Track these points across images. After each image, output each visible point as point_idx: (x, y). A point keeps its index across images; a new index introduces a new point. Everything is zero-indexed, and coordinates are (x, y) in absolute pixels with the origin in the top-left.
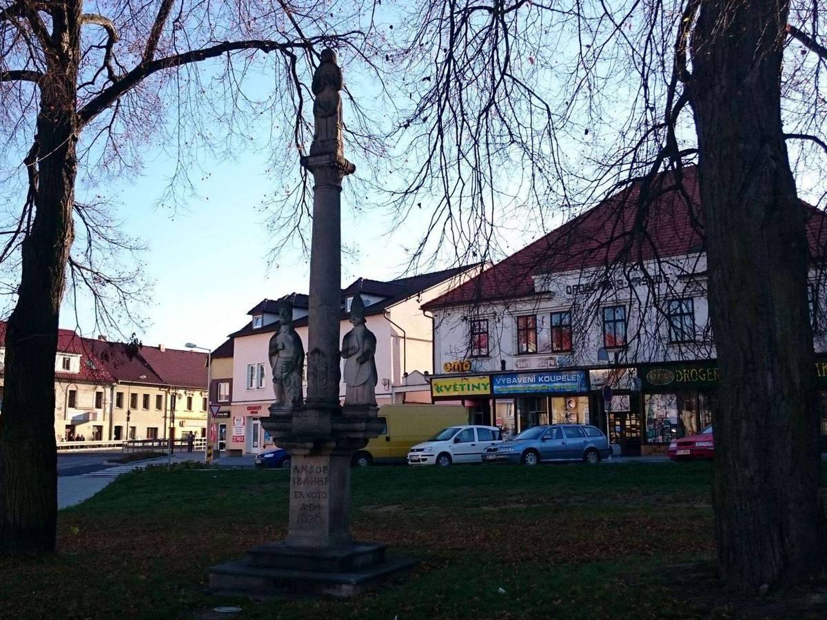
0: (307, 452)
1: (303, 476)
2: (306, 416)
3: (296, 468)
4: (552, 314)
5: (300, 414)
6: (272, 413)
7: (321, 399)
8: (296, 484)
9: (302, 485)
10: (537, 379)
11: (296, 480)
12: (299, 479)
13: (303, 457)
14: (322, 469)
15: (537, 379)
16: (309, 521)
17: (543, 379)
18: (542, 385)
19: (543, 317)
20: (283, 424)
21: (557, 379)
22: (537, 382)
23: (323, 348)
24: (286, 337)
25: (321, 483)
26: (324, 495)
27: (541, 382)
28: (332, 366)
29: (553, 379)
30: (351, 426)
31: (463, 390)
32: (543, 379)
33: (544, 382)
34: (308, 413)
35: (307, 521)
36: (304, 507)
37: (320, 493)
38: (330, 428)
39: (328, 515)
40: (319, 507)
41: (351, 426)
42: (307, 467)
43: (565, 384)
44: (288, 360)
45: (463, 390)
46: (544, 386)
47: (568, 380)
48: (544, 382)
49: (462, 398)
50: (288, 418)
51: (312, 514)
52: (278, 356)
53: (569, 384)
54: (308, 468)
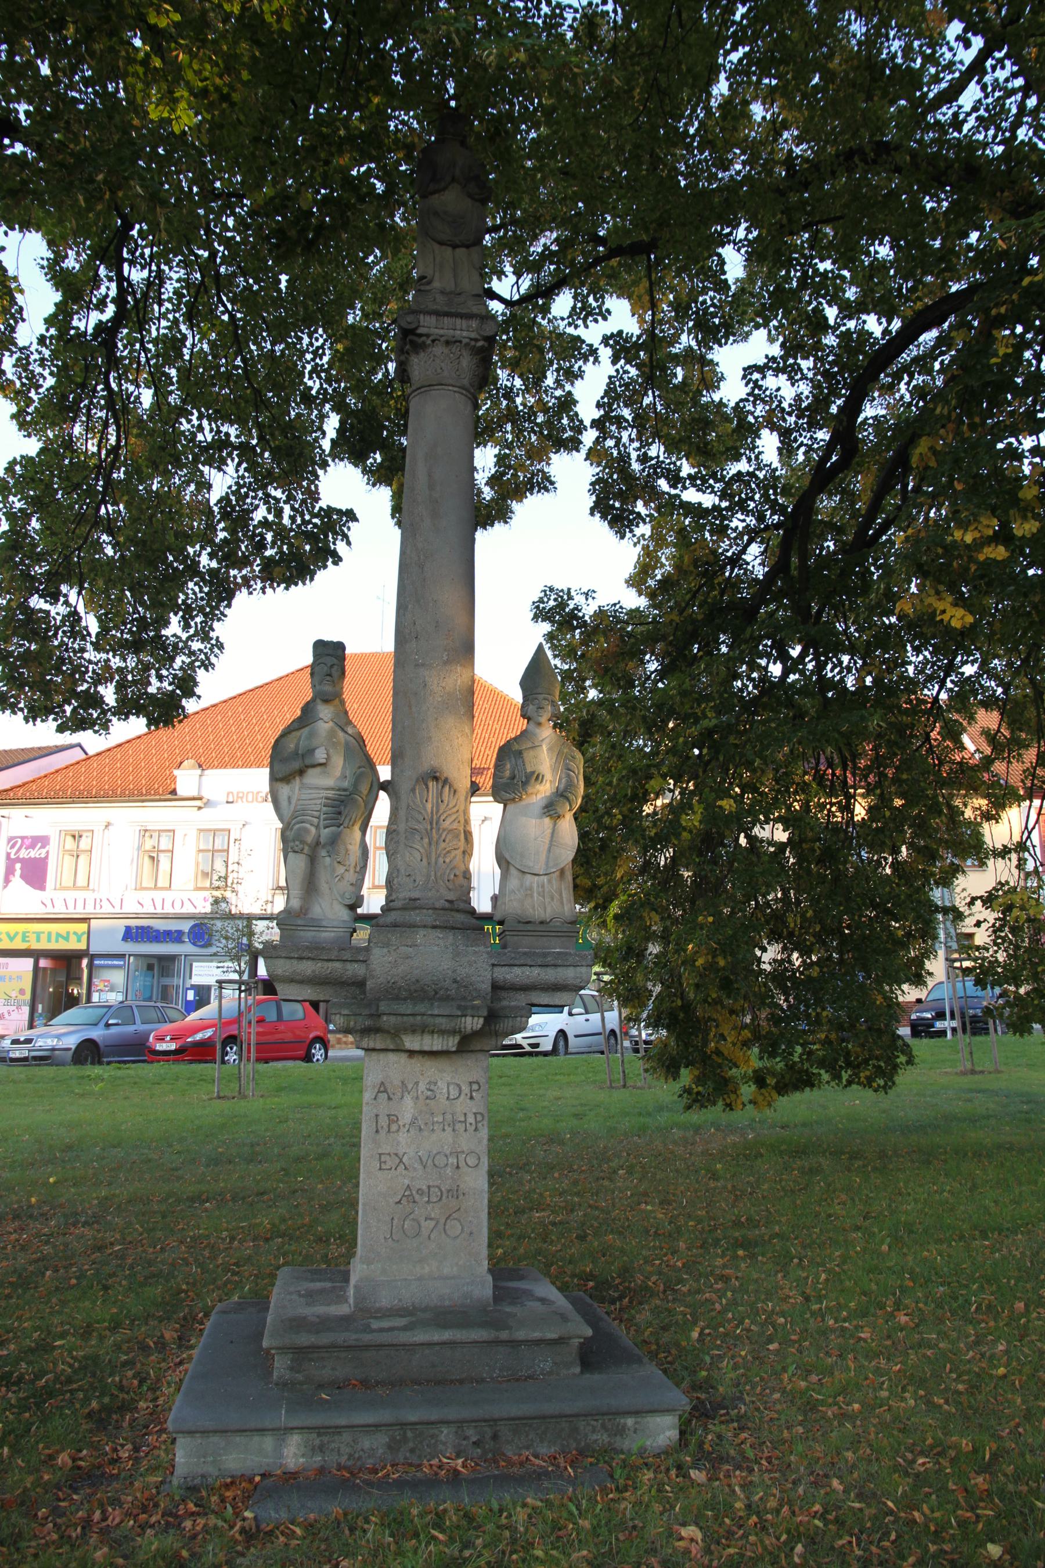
1: (407, 1108)
3: (382, 1088)
9: (403, 1137)
11: (383, 1122)
12: (392, 1119)
14: (466, 1089)
16: (425, 1232)
26: (472, 1161)
30: (550, 975)
31: (38, 940)
36: (409, 1196)
37: (457, 1154)
38: (489, 977)
42: (417, 1083)
45: (38, 940)
49: (35, 954)
54: (422, 1087)
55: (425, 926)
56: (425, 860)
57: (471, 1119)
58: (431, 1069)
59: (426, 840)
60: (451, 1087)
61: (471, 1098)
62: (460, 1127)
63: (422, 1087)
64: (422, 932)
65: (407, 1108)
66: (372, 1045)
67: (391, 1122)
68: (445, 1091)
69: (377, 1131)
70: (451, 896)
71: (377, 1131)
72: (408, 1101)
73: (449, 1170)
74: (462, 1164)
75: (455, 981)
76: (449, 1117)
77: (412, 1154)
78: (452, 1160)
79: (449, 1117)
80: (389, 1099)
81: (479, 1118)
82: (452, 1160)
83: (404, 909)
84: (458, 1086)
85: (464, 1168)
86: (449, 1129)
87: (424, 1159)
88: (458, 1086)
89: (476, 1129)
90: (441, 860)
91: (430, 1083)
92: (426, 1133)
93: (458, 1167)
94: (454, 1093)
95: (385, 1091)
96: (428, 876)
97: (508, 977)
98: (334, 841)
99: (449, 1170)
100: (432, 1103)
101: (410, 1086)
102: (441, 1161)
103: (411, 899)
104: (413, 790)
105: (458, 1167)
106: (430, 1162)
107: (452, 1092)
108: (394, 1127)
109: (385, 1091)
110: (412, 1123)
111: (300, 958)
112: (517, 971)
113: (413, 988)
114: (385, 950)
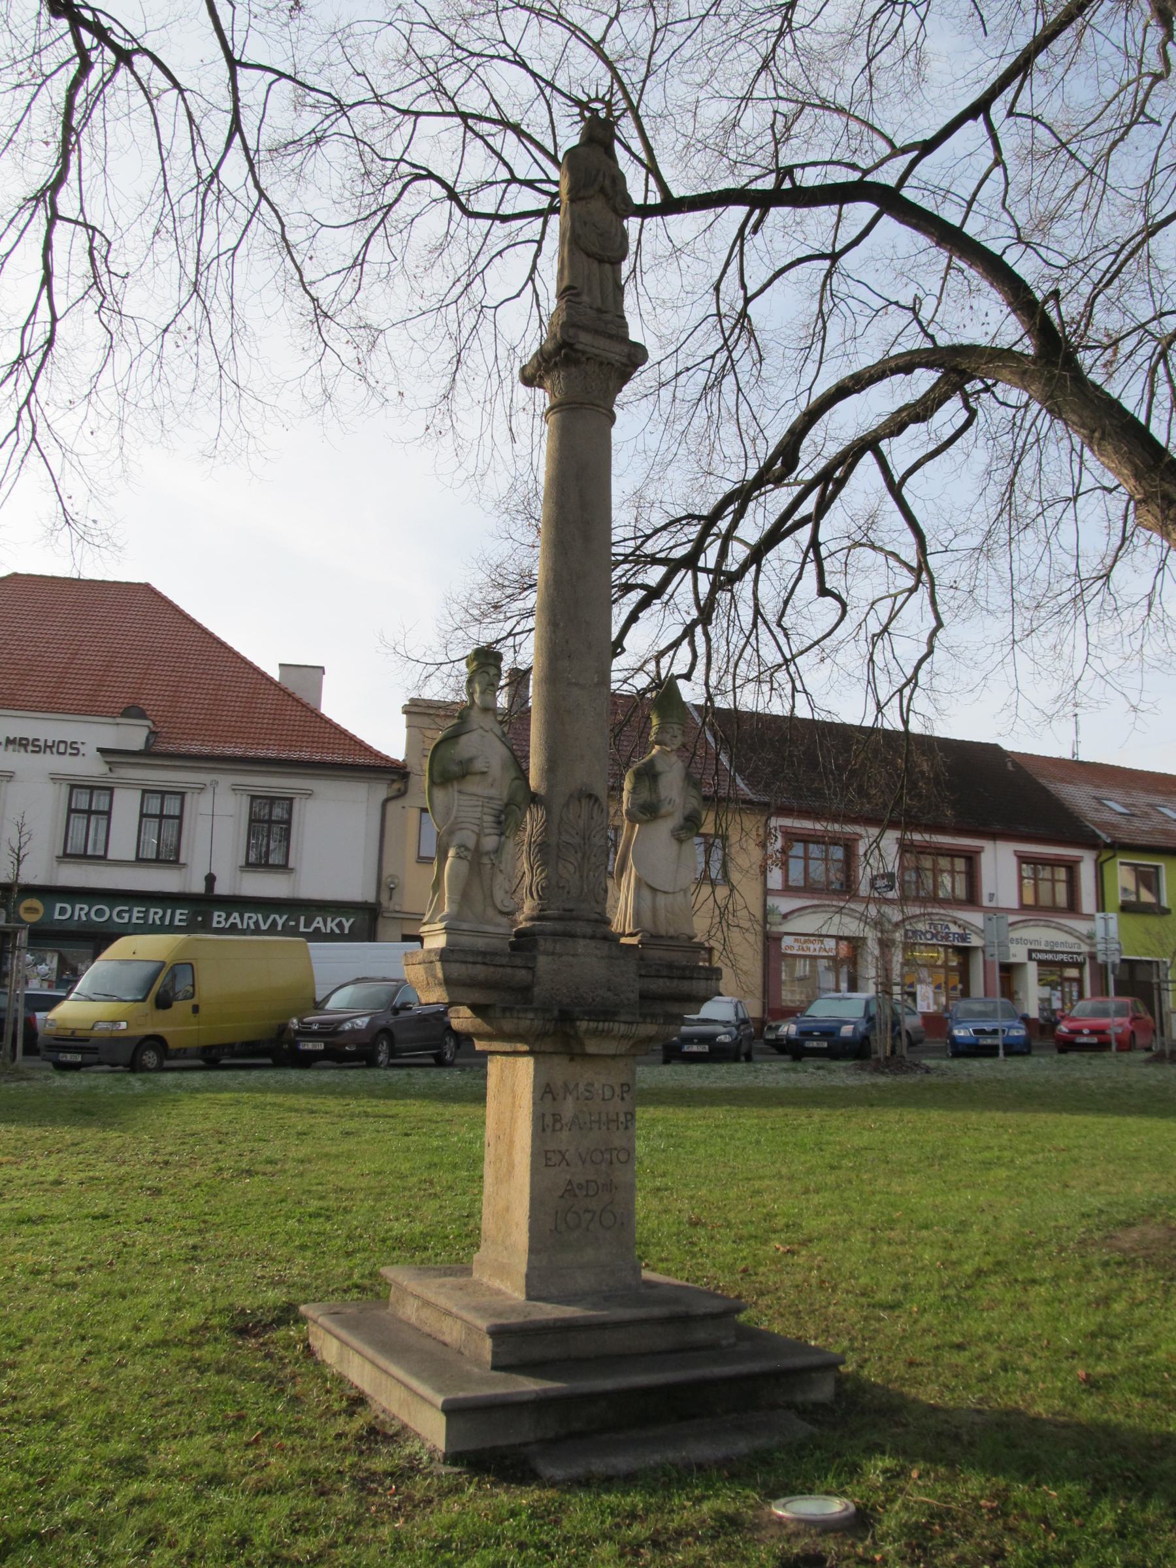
1: (568, 1108)
8: (549, 1131)
9: (565, 1135)
11: (549, 1120)
12: (556, 1118)
14: (618, 1091)
25: (613, 1126)
26: (623, 1157)
37: (610, 1150)
42: (577, 1085)
54: (581, 1088)
55: (584, 937)
57: (622, 1119)
59: (580, 855)
62: (613, 1126)
63: (581, 1088)
64: (582, 942)
65: (568, 1108)
66: (543, 1048)
67: (555, 1121)
72: (570, 1099)
73: (604, 1167)
76: (604, 1118)
79: (604, 1118)
83: (560, 919)
89: (626, 1128)
94: (608, 1094)
95: (551, 1092)
99: (604, 1167)
101: (571, 1087)
104: (567, 805)
108: (558, 1126)
109: (551, 1092)
111: (474, 963)
112: (661, 981)
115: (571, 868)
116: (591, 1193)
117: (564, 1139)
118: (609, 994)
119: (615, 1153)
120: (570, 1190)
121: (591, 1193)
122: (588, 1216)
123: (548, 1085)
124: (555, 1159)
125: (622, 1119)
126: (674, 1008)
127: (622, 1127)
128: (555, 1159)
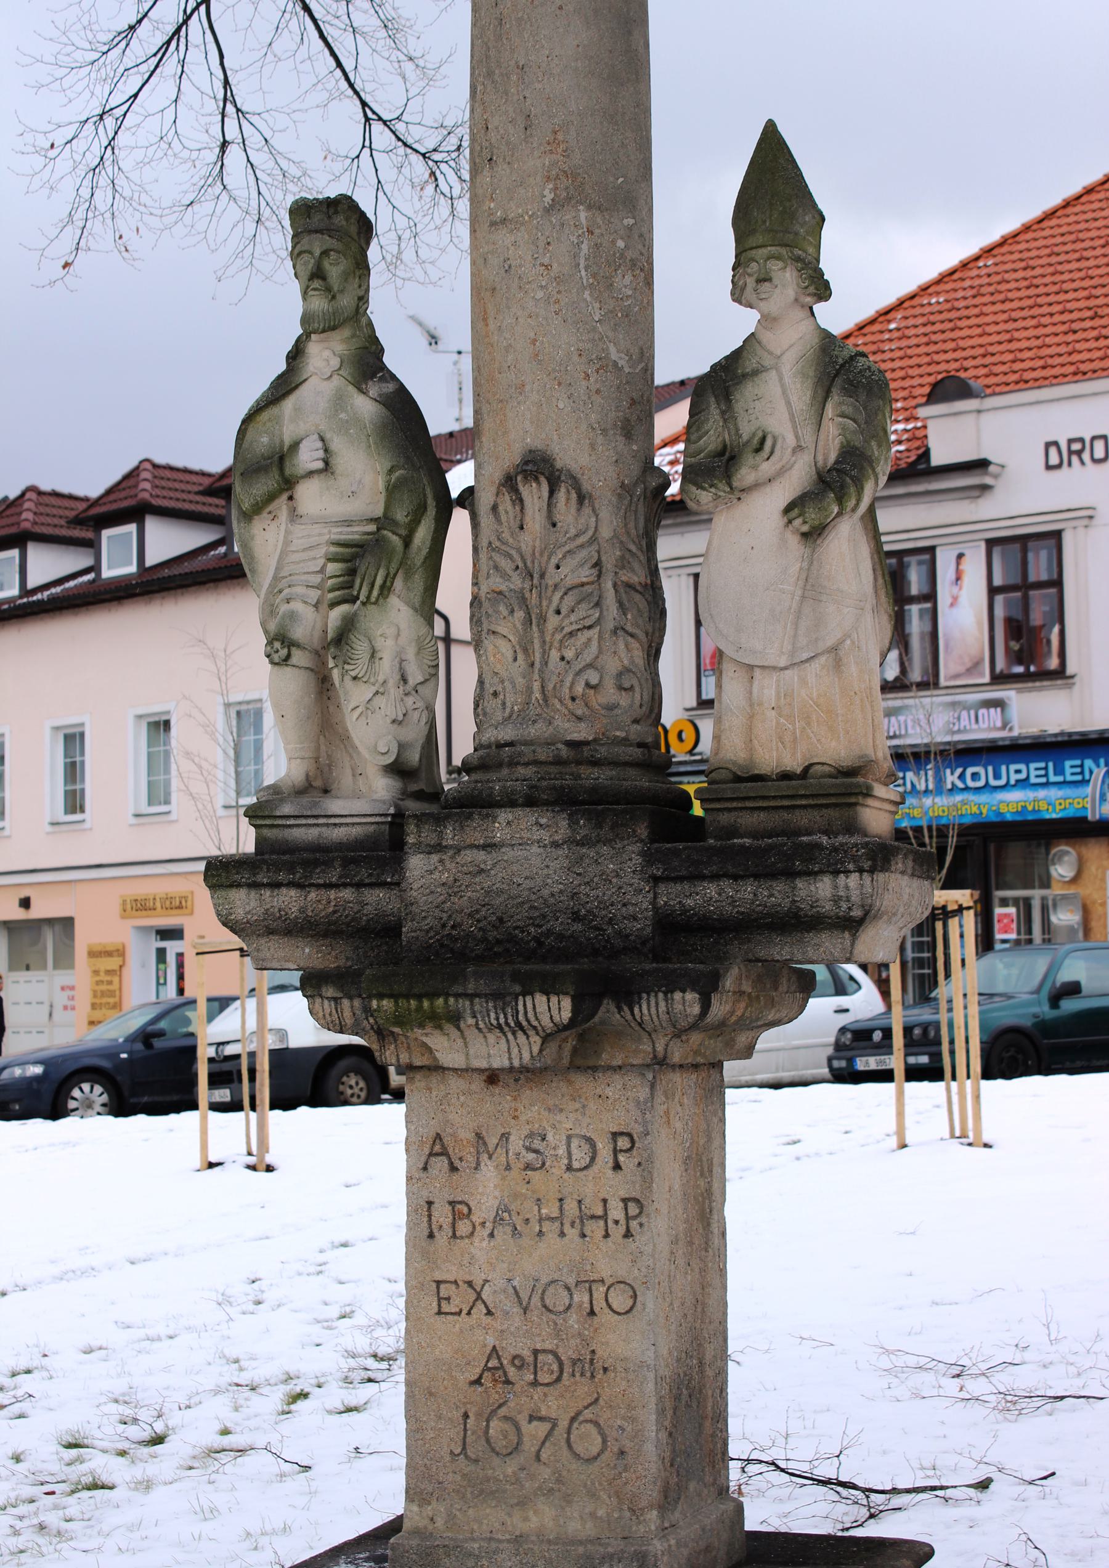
0: (525, 1050)
1: (487, 1188)
2: (489, 847)
4: (991, 543)
5: (450, 835)
6: (267, 833)
7: (572, 744)
8: (442, 1238)
9: (480, 1246)
10: (940, 780)
11: (442, 1215)
12: (460, 1210)
13: (478, 1084)
15: (940, 780)
17: (962, 777)
18: (959, 798)
19: (960, 556)
20: (347, 894)
21: (1014, 778)
22: (939, 790)
23: (578, 450)
24: (339, 401)
25: (595, 1229)
26: (620, 1300)
27: (954, 789)
28: (622, 564)
29: (997, 776)
30: (774, 895)
32: (962, 777)
33: (967, 789)
34: (504, 824)
35: (517, 1448)
37: (590, 1285)
39: (649, 1420)
40: (590, 1366)
41: (774, 895)
42: (505, 1137)
43: (1042, 793)
44: (354, 533)
46: (964, 803)
47: (1053, 778)
48: (967, 789)
50: (381, 851)
51: (553, 1405)
52: (294, 515)
53: (1053, 793)
54: (516, 1143)
56: (520, 657)
57: (616, 1212)
58: (532, 1109)
59: (520, 614)
60: (575, 1143)
61: (617, 1167)
62: (595, 1229)
63: (516, 1143)
64: (504, 816)
65: (487, 1188)
67: (457, 1217)
68: (562, 1151)
69: (431, 1236)
70: (581, 732)
71: (431, 1236)
72: (489, 1171)
74: (599, 1304)
75: (576, 917)
76: (571, 1207)
77: (501, 1283)
78: (581, 1297)
79: (571, 1207)
80: (453, 1169)
81: (633, 1210)
82: (581, 1297)
84: (589, 1140)
85: (605, 1317)
86: (572, 1233)
87: (525, 1296)
88: (589, 1140)
89: (628, 1234)
90: (554, 655)
91: (531, 1135)
92: (525, 1241)
93: (592, 1313)
94: (580, 1157)
95: (444, 1153)
96: (529, 690)
97: (690, 902)
98: (347, 627)
100: (535, 1176)
101: (492, 1141)
102: (558, 1298)
103: (500, 746)
105: (592, 1313)
106: (536, 1299)
107: (576, 1154)
108: (463, 1228)
109: (444, 1153)
110: (498, 1220)
112: (711, 890)
113: (493, 935)
114: (435, 858)
115: (506, 650)
116: (544, 1378)
117: (482, 1257)
118: (578, 927)
119: (599, 1291)
120: (495, 1370)
121: (544, 1378)
122: (543, 1428)
123: (438, 1137)
124: (460, 1299)
125: (616, 1212)
126: (780, 950)
127: (617, 1232)
128: (460, 1299)
